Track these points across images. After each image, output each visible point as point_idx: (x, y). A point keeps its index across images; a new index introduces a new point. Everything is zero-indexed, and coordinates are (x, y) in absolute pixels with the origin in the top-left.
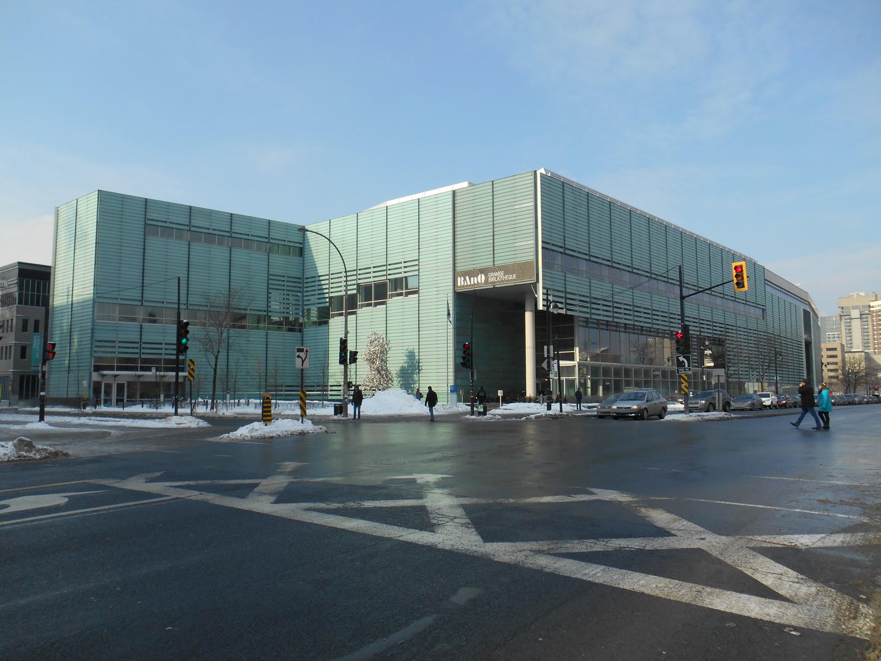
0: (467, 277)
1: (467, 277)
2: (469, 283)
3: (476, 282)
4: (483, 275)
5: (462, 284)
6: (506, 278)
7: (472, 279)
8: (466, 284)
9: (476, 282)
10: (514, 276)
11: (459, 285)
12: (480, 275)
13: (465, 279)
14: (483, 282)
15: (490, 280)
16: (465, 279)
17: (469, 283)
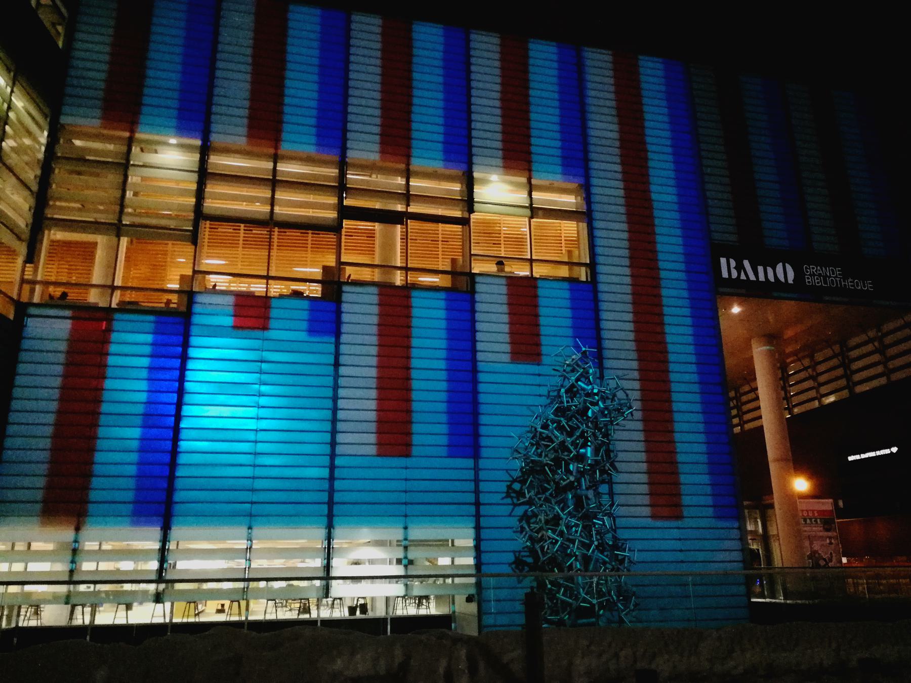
0: (746, 263)
1: (746, 263)
2: (752, 277)
3: (772, 279)
4: (789, 267)
5: (735, 274)
6: (849, 283)
7: (760, 269)
8: (743, 277)
9: (772, 279)
10: (868, 286)
11: (725, 274)
12: (779, 267)
13: (740, 267)
14: (790, 281)
15: (808, 280)
16: (740, 267)
17: (752, 277)
